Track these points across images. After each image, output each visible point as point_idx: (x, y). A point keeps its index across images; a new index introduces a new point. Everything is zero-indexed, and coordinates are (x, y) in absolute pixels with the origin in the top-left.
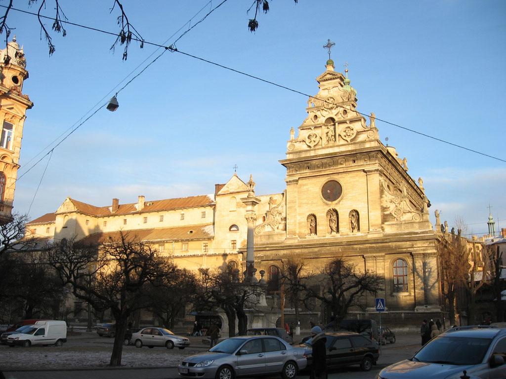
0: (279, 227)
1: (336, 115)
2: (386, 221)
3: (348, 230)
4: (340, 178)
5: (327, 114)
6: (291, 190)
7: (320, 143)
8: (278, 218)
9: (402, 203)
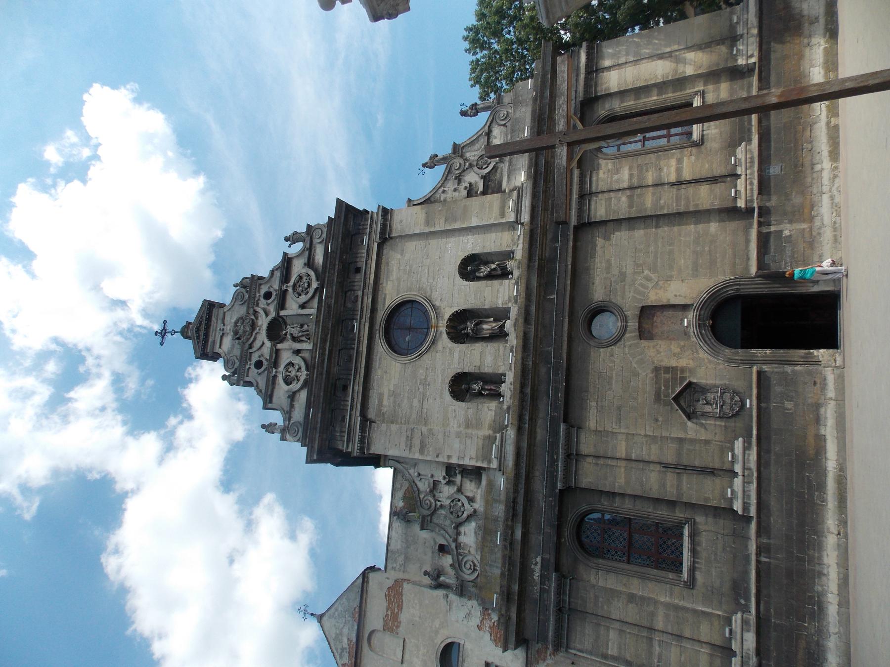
0: (470, 494)
1: (267, 315)
4: (384, 304)
5: (262, 336)
7: (307, 355)
8: (446, 492)
9: (468, 155)
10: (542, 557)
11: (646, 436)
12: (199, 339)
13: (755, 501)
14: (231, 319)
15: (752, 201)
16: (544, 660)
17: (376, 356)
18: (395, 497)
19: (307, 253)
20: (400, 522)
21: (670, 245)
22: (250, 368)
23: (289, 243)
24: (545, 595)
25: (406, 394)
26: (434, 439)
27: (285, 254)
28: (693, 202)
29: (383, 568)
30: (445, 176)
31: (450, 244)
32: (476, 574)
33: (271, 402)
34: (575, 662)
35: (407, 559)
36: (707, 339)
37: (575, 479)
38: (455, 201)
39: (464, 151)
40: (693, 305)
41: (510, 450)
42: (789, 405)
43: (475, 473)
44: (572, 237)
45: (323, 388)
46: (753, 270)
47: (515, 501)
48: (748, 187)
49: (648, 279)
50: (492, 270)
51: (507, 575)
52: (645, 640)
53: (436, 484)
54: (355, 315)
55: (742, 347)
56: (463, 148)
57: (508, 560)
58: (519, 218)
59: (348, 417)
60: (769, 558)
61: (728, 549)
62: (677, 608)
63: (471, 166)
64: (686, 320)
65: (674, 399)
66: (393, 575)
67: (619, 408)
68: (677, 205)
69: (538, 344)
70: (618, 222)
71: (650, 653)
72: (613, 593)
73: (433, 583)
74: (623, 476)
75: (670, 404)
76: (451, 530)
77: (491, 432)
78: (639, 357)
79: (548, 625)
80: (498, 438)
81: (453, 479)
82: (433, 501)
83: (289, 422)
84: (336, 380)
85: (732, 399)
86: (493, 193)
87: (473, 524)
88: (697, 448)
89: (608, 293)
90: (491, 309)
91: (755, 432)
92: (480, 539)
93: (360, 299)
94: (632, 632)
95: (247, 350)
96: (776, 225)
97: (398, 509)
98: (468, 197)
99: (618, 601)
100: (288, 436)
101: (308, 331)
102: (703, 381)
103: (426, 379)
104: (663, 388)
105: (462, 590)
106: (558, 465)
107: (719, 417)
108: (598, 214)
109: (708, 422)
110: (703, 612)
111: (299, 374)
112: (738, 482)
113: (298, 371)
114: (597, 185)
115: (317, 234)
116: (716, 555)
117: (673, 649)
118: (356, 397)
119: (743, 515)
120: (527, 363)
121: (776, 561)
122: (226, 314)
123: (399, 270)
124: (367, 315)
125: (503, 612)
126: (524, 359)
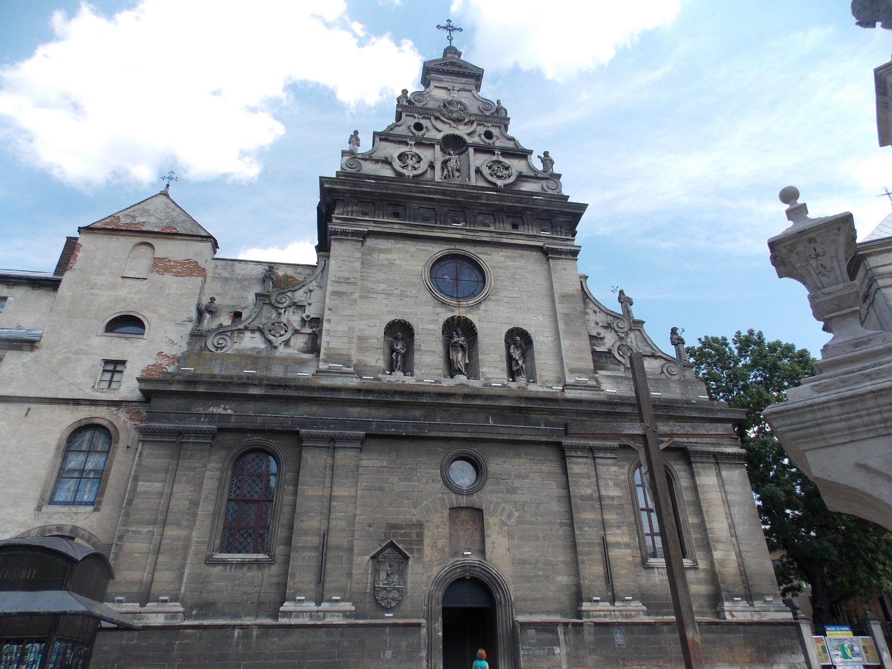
0: (292, 341)
1: (469, 134)
2: (601, 369)
3: (505, 375)
4: (480, 253)
5: (447, 130)
6: (343, 254)
7: (429, 175)
8: (294, 318)
9: (632, 335)
10: (232, 415)
11: (355, 516)
12: (444, 65)
13: (293, 623)
14: (464, 98)
15: (588, 616)
16: (130, 419)
17: (429, 246)
18: (288, 267)
19: (532, 174)
20: (262, 273)
21: (544, 537)
22: (415, 118)
23: (543, 156)
24: (195, 419)
25: (391, 277)
26: (347, 306)
27: (531, 152)
28: (588, 560)
29: (216, 256)
30: (611, 313)
31: (542, 319)
32: (213, 349)
33: (381, 140)
34: (129, 449)
35: (226, 280)
36: (451, 573)
37: (310, 446)
38: (585, 323)
39: (636, 332)
40: (485, 560)
41: (339, 382)
42: (389, 654)
43: (314, 348)
44: (550, 440)
45: (396, 193)
46: (521, 618)
47: (286, 387)
48: (602, 613)
49: (510, 516)
50: (517, 361)
51: (213, 381)
52: (153, 518)
53: (302, 307)
54: (470, 225)
55: (444, 609)
56: (639, 330)
57: (227, 382)
58: (569, 387)
59: (367, 218)
60: (238, 637)
61: (245, 597)
62: (186, 548)
63: (621, 339)
64: (470, 553)
65: (391, 541)
66: (210, 267)
67: (381, 489)
68: (583, 543)
69: (444, 408)
70: (567, 486)
71: (140, 523)
72: (199, 485)
73: (203, 307)
74: (315, 494)
75: (386, 539)
76: (256, 324)
77: (355, 362)
78: (432, 508)
79: (166, 422)
80: (349, 369)
81: (307, 325)
82: (284, 305)
83: (361, 159)
84: (404, 206)
85: (393, 599)
86: (594, 361)
87: (263, 346)
88: (344, 566)
89: (496, 477)
90: (477, 361)
91: (361, 622)
92: (248, 353)
93: (486, 229)
94: (161, 504)
95: (433, 115)
96: (565, 640)
97: (276, 271)
98: (590, 336)
99: (191, 491)
100: (347, 158)
101: (453, 176)
102: (409, 571)
103: (407, 296)
104: (402, 531)
105: (197, 336)
106: (323, 428)
107: (375, 587)
108: (573, 466)
109: (370, 576)
110: (183, 573)
111: (410, 168)
112: (311, 606)
113: (412, 167)
114: (603, 465)
115: (551, 184)
116: (239, 585)
117: (145, 545)
118: (387, 226)
119: (279, 611)
120: (424, 397)
121: (235, 643)
122: (470, 93)
123: (516, 268)
124: (470, 236)
125: (177, 377)
126: (428, 394)
